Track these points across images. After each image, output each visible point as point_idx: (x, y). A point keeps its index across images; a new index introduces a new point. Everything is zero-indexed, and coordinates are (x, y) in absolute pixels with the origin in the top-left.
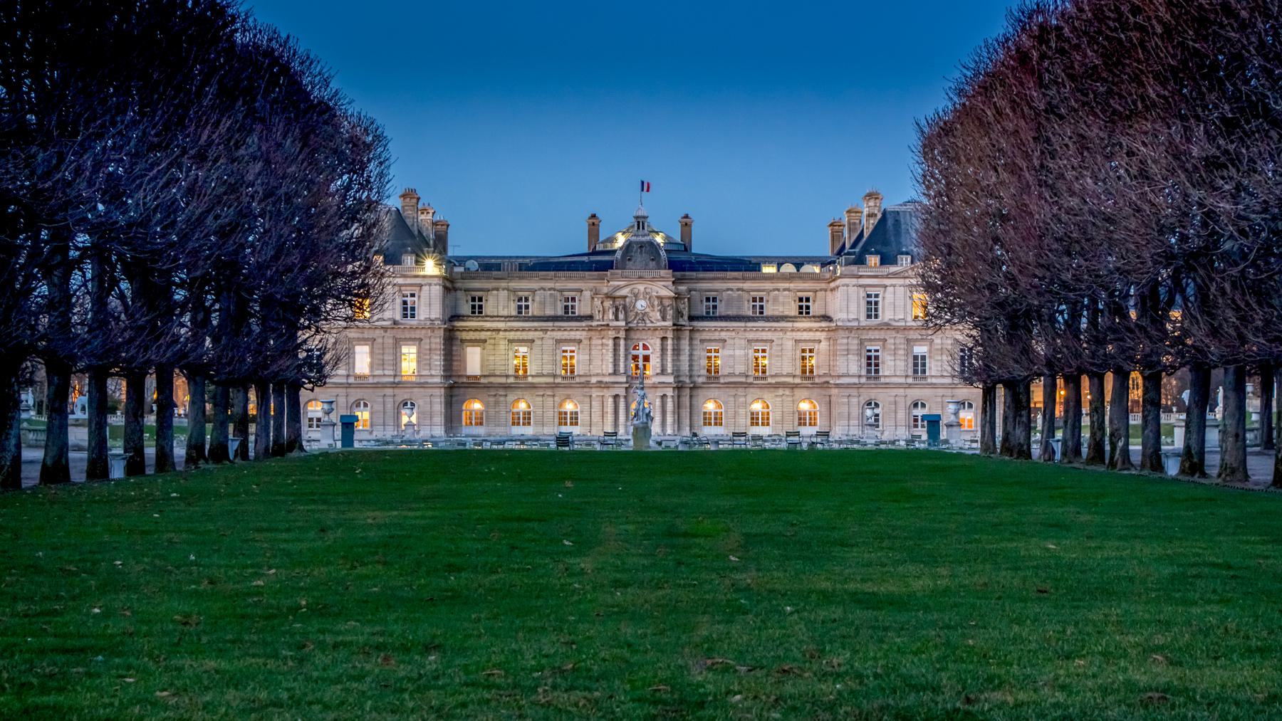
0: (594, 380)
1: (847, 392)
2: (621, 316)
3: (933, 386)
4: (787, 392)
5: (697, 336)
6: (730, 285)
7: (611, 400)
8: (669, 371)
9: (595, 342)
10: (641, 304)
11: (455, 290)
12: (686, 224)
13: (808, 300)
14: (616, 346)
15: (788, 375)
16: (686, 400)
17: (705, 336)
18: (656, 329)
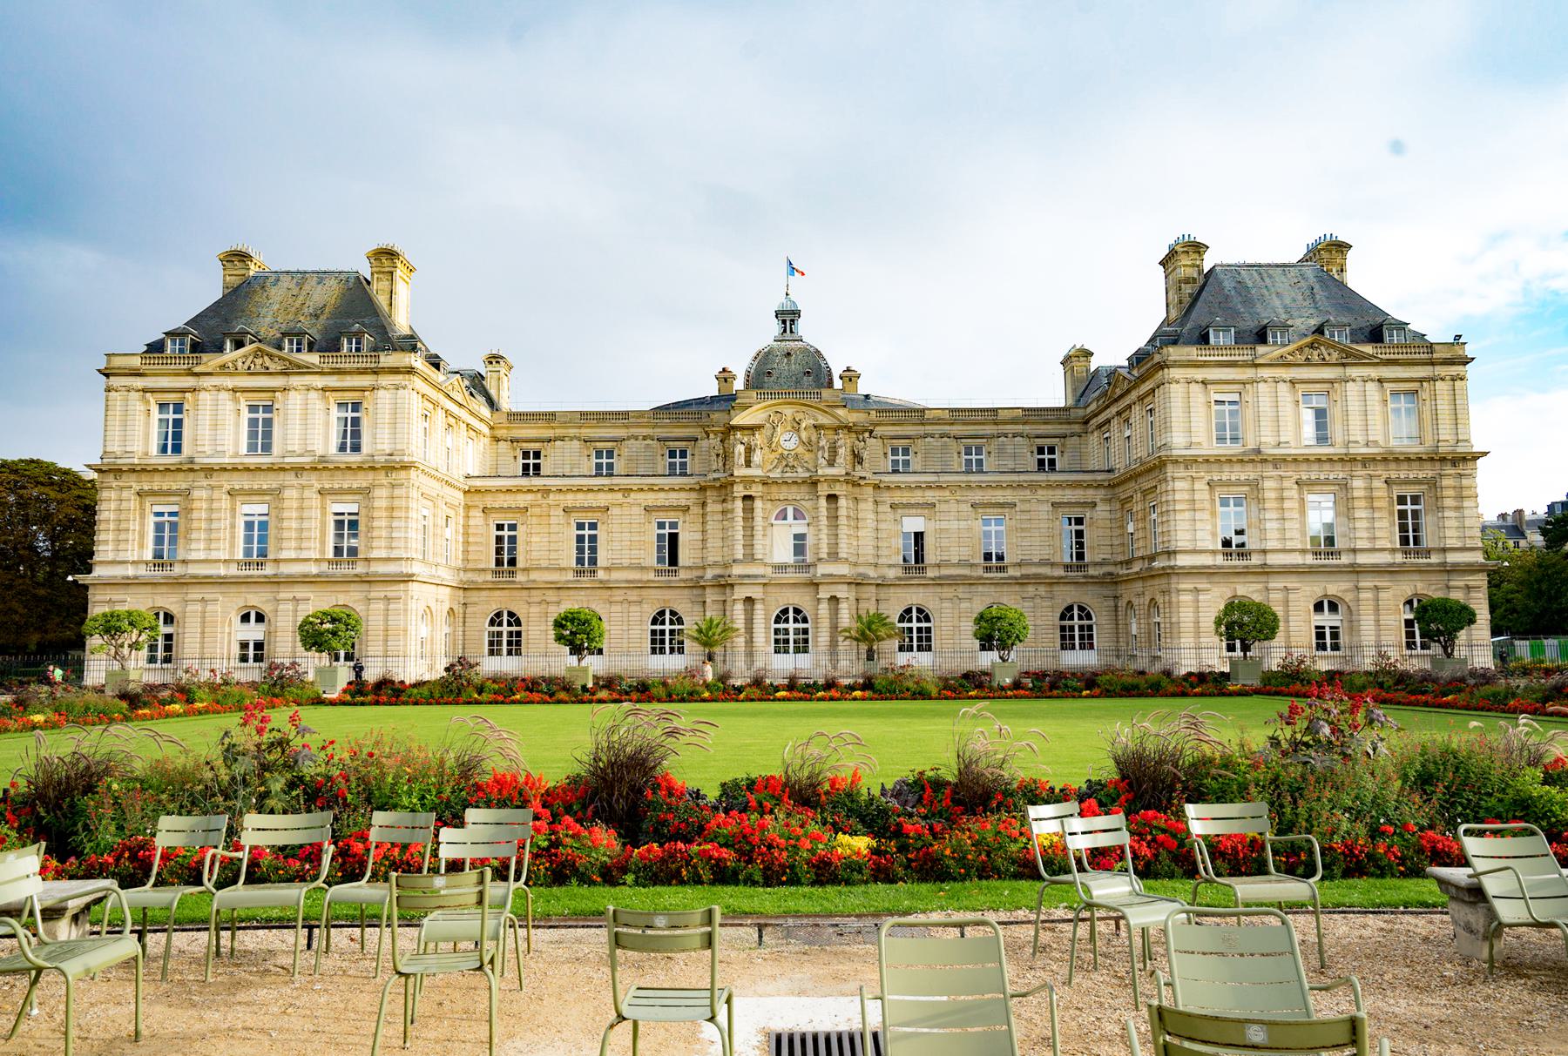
0: (709, 574)
1: (1186, 584)
2: (757, 457)
3: (1355, 570)
4: (1042, 590)
5: (886, 497)
6: (929, 429)
7: (739, 607)
9: (712, 507)
10: (788, 442)
13: (1052, 450)
15: (1042, 563)
17: (898, 497)
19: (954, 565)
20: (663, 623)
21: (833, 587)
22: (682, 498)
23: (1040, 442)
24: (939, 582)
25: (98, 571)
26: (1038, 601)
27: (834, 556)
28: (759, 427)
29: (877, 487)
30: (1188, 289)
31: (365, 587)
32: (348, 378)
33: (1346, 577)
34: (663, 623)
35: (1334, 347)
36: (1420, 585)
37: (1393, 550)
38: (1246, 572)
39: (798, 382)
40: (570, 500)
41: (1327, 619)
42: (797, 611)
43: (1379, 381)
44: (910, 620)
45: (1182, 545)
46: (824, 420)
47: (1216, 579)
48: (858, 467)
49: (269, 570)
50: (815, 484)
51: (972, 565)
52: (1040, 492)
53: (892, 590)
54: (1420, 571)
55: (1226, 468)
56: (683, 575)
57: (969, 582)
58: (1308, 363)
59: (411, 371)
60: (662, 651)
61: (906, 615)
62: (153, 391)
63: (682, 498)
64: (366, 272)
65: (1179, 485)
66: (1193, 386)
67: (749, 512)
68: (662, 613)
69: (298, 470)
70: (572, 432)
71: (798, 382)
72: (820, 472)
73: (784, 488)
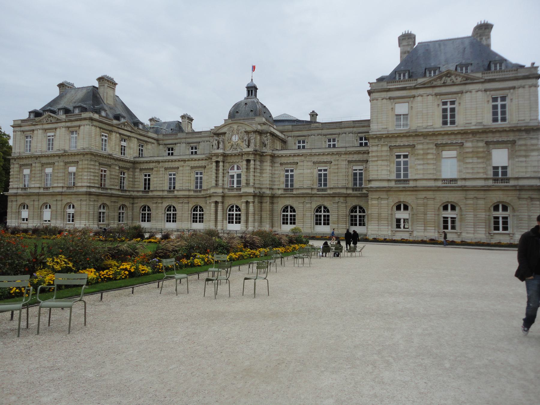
2: (221, 146)
3: (464, 189)
4: (342, 199)
5: (279, 160)
6: (313, 132)
7: (213, 205)
8: (251, 184)
10: (235, 139)
11: (159, 144)
12: (314, 115)
14: (217, 166)
16: (267, 205)
17: (284, 160)
18: (241, 155)
19: (304, 189)
20: (197, 211)
21: (247, 197)
22: (203, 163)
23: (360, 135)
24: (298, 196)
25: (11, 191)
26: (340, 204)
27: (248, 184)
28: (225, 133)
29: (273, 156)
30: (405, 56)
31: (76, 196)
32: (73, 123)
33: (459, 193)
34: (197, 211)
35: (459, 75)
36: (502, 196)
37: (486, 179)
38: (404, 190)
39: (248, 115)
40: (167, 165)
41: (449, 214)
42: (237, 207)
43: (486, 91)
44: (287, 212)
45: (375, 177)
46: (249, 129)
47: (391, 193)
48: (264, 148)
49: (51, 190)
50: (242, 155)
51: (312, 189)
52: (343, 156)
53: (279, 199)
54: (500, 189)
55: (399, 140)
56: (203, 193)
57: (312, 196)
58: (445, 85)
59: (91, 119)
60: (196, 222)
61: (285, 209)
62: (23, 132)
63: (203, 163)
64: (97, 85)
65: (375, 149)
66: (385, 101)
67: (217, 166)
68: (197, 207)
69: (59, 156)
70: (183, 140)
71: (248, 115)
72: (244, 150)
73: (233, 158)
